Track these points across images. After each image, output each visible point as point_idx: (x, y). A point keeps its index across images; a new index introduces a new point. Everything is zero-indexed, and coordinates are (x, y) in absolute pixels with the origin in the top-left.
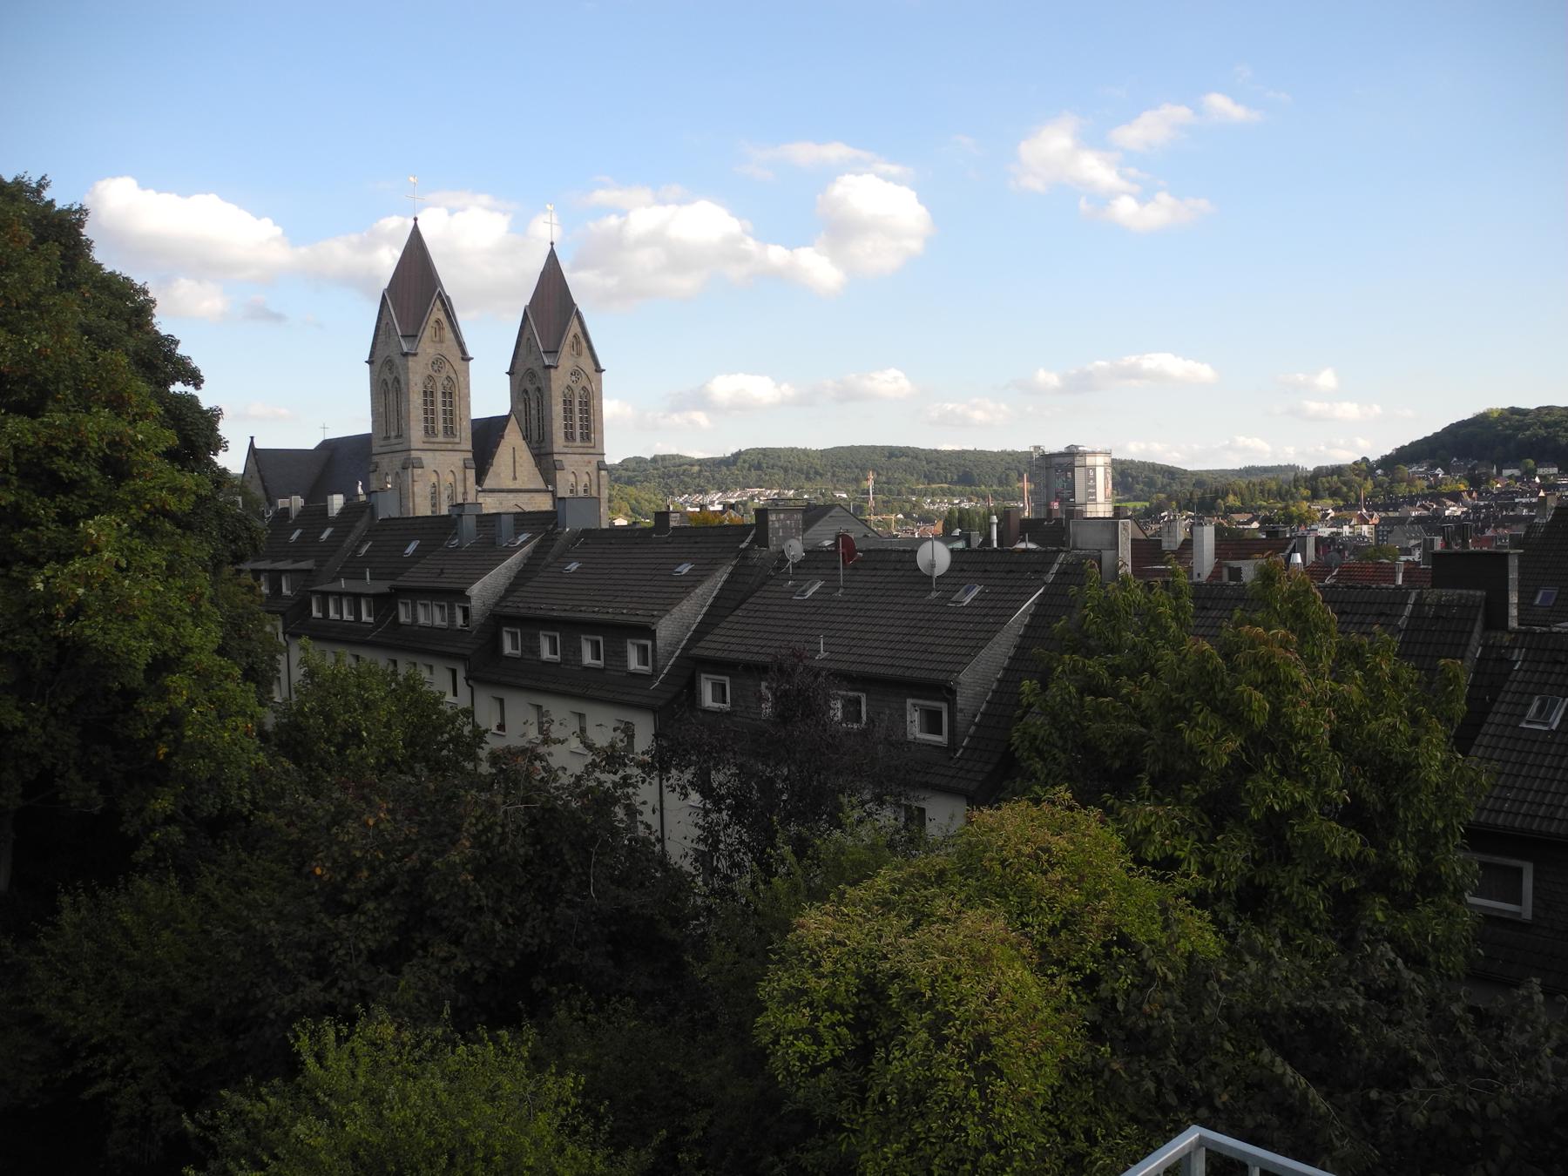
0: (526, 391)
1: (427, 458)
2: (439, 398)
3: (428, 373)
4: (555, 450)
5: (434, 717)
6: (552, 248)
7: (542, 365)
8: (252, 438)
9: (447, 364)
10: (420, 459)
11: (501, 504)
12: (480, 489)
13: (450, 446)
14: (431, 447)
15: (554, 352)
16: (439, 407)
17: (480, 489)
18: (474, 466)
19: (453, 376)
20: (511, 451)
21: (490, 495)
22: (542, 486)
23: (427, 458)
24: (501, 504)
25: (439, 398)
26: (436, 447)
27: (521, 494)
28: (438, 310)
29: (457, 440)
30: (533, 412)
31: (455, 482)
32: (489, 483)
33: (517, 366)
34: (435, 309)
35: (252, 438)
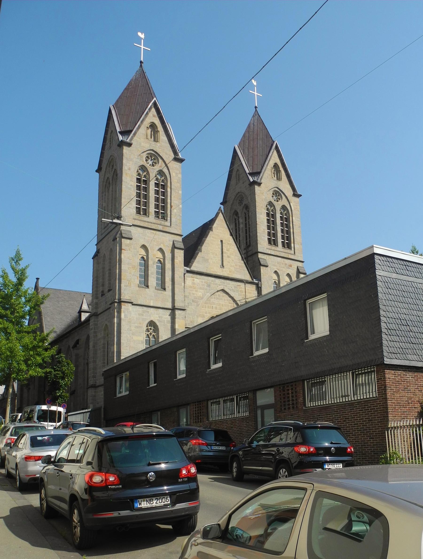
0: (236, 213)
1: (135, 232)
2: (152, 188)
3: (142, 163)
4: (260, 250)
5: (12, 370)
6: (256, 110)
7: (248, 183)
8: (38, 279)
9: (160, 160)
10: (130, 232)
11: (209, 286)
12: (188, 269)
13: (160, 228)
14: (142, 224)
15: (257, 174)
16: (152, 195)
17: (188, 269)
18: (182, 247)
19: (165, 170)
20: (220, 243)
21: (198, 276)
22: (248, 278)
23: (135, 232)
24: (209, 286)
25: (152, 188)
26: (146, 225)
27: (228, 281)
28: (154, 116)
29: (168, 223)
30: (241, 226)
31: (164, 259)
32: (196, 266)
33: (229, 195)
34: (150, 114)
35: (38, 279)
